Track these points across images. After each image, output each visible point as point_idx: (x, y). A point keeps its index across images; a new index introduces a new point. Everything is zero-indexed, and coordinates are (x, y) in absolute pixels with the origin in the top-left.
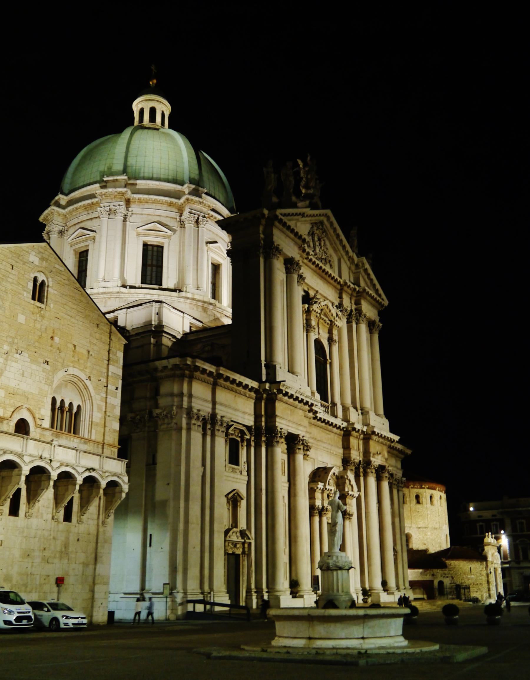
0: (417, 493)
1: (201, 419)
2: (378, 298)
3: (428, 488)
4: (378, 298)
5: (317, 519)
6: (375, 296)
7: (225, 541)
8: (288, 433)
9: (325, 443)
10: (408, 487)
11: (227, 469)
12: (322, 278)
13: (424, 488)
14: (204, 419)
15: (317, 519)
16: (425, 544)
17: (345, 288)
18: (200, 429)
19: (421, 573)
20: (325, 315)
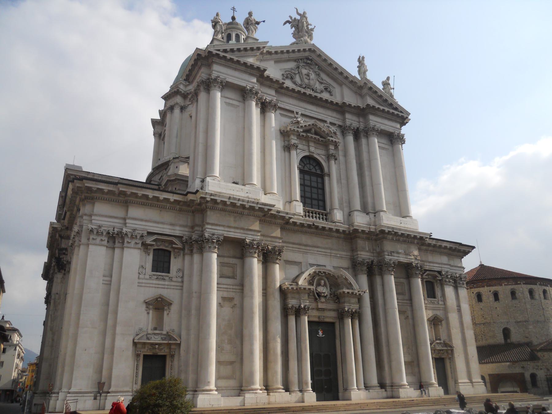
0: (512, 289)
1: (105, 233)
2: (396, 112)
3: (524, 284)
4: (396, 112)
5: (292, 320)
6: (391, 111)
7: (135, 344)
8: (224, 236)
9: (318, 247)
10: (501, 285)
11: (147, 277)
12: (313, 104)
13: (520, 284)
14: (108, 233)
15: (292, 320)
16: (527, 337)
17: (347, 109)
18: (105, 243)
19: (509, 366)
20: (316, 133)
